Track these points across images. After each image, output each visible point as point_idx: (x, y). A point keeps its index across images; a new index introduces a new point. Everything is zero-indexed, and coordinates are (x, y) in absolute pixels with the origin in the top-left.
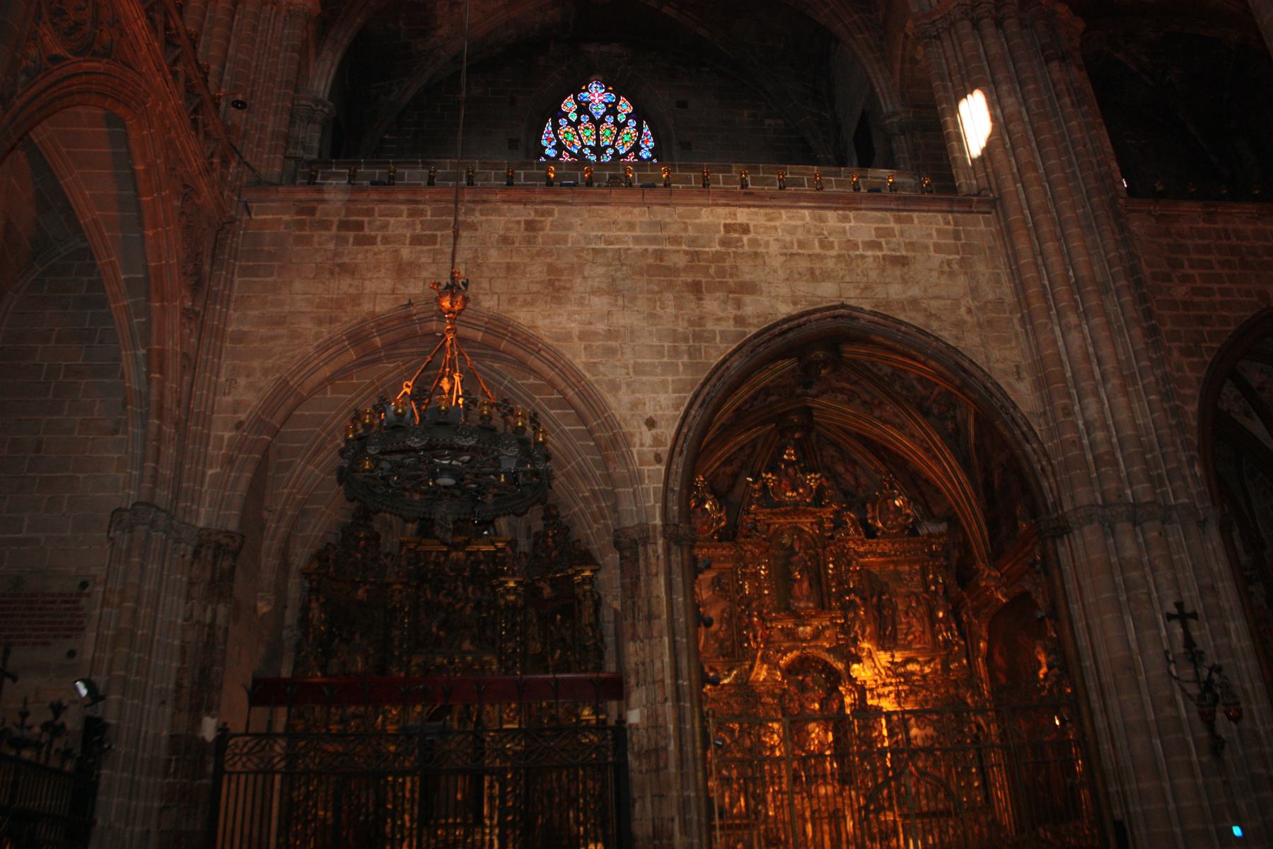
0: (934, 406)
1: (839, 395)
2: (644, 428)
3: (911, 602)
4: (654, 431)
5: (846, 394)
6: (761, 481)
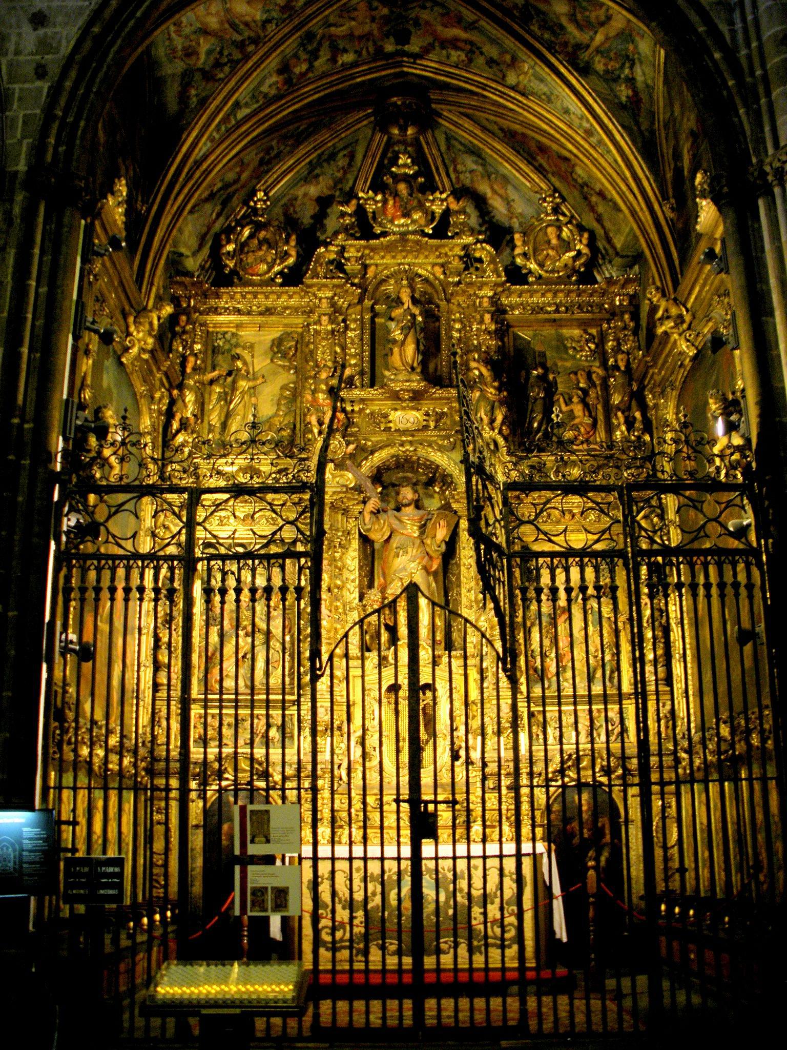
0: (597, 59)
1: (453, 53)
2: (27, 28)
3: (579, 382)
4: (41, 32)
5: (462, 50)
6: (354, 202)
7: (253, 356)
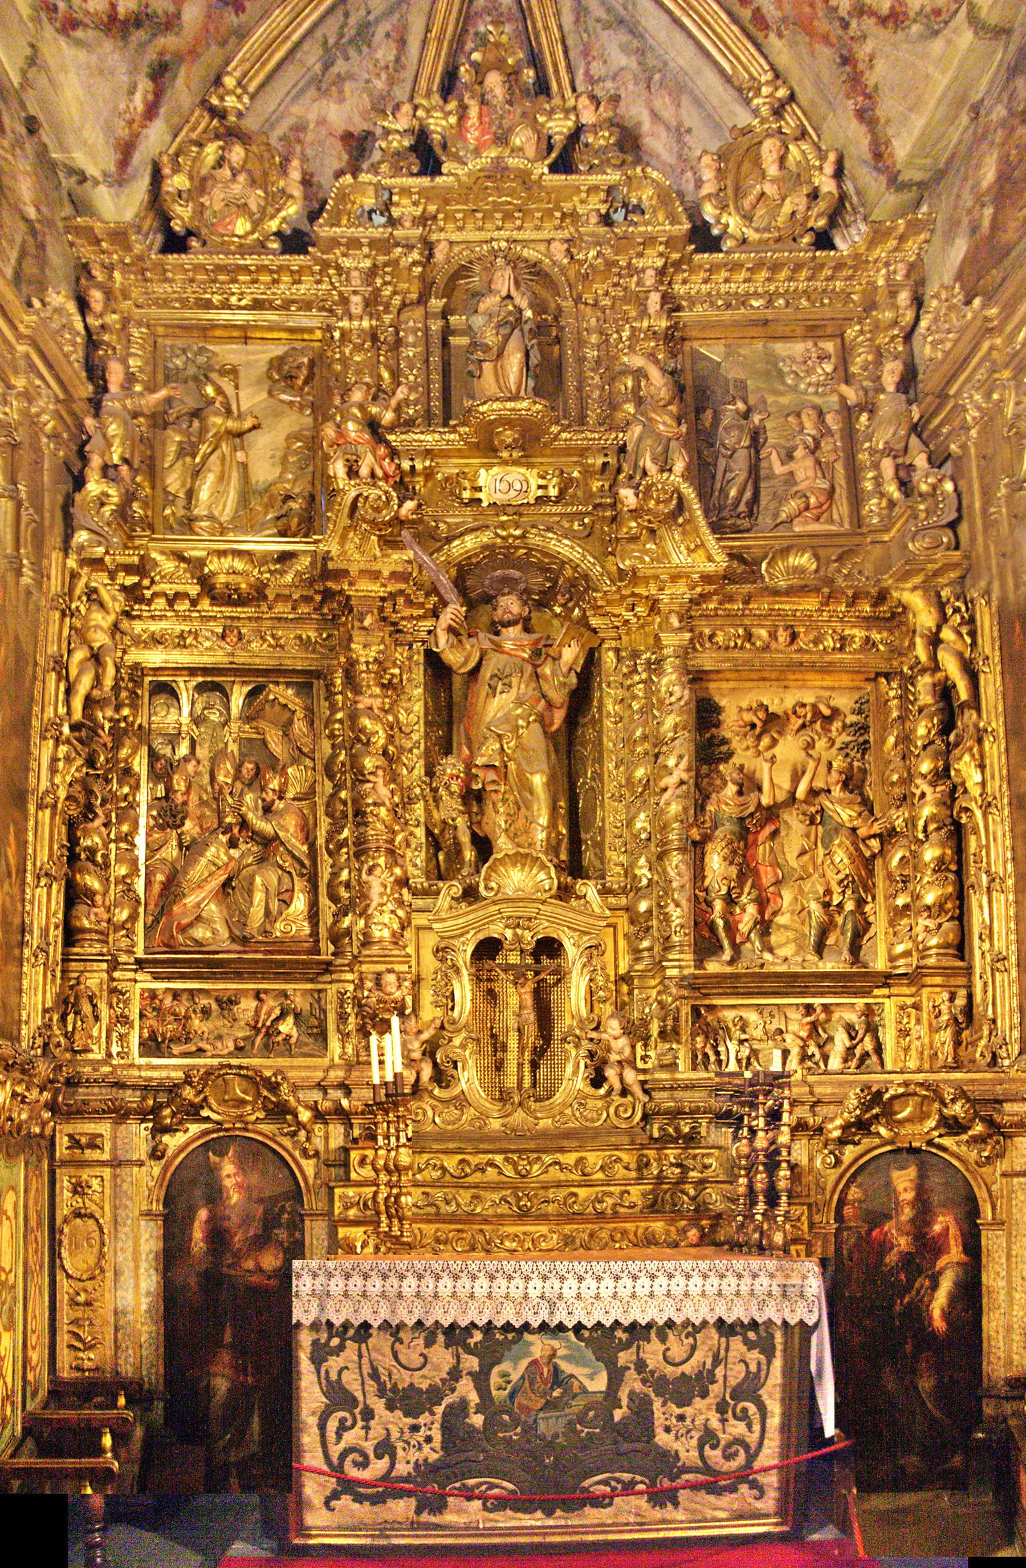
7: (237, 387)
